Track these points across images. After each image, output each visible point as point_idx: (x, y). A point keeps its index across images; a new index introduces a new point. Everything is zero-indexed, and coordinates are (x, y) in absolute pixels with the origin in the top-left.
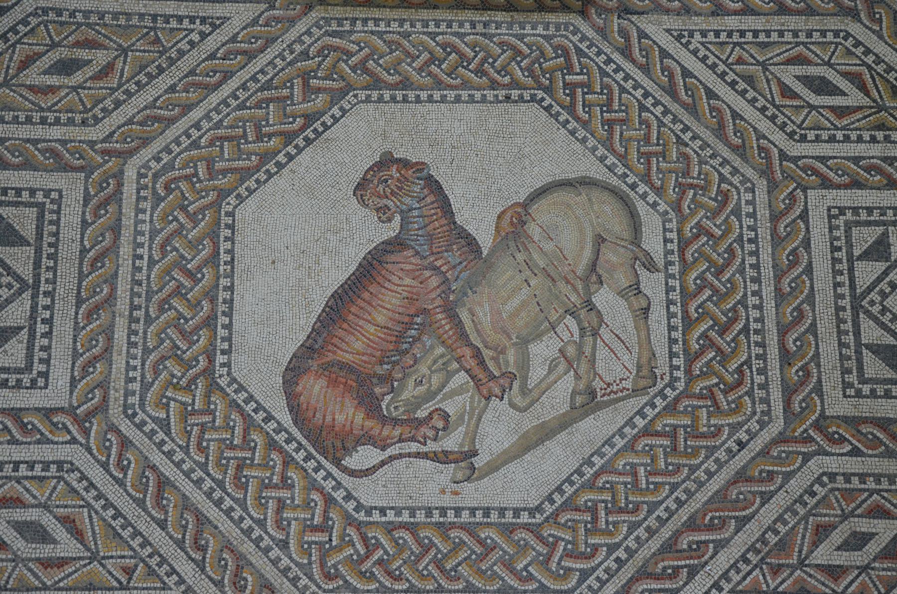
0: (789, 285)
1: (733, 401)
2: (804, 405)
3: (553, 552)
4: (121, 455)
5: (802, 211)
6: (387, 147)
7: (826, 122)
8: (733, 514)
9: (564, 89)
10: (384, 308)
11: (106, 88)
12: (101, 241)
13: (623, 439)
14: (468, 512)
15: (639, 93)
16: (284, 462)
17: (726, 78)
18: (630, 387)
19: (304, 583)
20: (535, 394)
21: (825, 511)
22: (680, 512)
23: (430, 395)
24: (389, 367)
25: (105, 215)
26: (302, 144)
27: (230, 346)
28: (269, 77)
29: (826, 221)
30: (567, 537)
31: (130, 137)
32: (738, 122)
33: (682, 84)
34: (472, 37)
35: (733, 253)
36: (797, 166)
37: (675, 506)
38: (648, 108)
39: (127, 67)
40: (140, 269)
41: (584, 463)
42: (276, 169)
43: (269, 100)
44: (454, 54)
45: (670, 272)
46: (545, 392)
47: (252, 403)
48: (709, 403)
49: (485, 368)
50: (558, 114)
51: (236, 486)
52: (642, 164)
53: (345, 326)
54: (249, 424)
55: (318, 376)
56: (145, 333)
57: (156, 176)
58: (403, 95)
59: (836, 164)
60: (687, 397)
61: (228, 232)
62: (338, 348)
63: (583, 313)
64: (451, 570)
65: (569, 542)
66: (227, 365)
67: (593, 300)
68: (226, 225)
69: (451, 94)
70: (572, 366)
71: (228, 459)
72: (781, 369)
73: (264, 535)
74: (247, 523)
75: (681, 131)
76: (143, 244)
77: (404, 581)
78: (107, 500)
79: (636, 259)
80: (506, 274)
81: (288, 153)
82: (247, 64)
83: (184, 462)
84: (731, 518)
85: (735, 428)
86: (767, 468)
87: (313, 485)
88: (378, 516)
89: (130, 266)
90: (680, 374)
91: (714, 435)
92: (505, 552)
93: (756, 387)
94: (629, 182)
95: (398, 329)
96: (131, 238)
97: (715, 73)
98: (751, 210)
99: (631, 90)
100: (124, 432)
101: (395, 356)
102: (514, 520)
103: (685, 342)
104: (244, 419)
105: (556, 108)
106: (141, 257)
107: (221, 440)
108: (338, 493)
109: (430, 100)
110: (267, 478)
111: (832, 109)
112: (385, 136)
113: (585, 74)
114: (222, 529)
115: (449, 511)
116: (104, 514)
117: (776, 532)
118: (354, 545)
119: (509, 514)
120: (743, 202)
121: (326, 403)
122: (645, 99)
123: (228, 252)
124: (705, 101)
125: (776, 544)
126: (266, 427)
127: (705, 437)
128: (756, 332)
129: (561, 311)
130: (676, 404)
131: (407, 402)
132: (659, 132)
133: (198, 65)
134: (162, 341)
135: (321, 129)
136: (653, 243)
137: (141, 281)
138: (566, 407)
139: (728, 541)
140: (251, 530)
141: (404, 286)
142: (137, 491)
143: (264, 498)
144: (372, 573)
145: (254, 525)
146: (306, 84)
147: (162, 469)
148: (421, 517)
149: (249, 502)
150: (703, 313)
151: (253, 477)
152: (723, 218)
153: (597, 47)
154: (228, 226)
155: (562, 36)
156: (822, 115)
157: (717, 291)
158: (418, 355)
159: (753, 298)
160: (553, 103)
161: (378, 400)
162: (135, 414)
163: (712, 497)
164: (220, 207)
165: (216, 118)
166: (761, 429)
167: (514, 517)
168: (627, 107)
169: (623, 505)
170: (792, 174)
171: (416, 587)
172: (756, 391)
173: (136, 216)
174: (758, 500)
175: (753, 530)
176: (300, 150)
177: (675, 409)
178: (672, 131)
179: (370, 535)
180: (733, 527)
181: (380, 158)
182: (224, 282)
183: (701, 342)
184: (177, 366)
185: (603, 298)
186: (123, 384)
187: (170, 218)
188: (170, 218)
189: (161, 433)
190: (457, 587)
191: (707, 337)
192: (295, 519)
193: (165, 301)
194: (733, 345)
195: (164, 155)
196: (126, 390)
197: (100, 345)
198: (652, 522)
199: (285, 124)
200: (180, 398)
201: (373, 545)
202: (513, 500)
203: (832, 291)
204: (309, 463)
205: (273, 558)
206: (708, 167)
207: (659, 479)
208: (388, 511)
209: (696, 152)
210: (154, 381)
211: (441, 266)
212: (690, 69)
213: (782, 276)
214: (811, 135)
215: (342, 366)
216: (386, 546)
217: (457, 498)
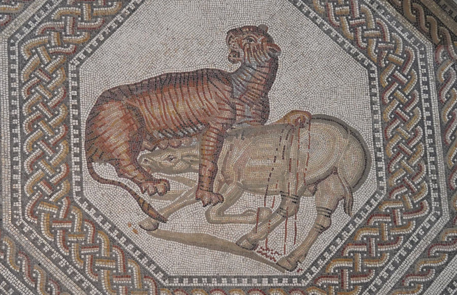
0: (410, 283)
5: (453, 251)
6: (269, 24)
9: (389, 77)
13: (248, 283)
14: (133, 247)
16: (64, 136)
18: (277, 260)
19: (17, 205)
20: (224, 219)
23: (169, 171)
24: (162, 137)
27: (92, 53)
34: (366, 7)
35: (398, 240)
38: (424, 126)
41: (216, 277)
44: (348, 7)
45: (355, 220)
46: (230, 222)
47: (76, 92)
49: (211, 183)
50: (374, 86)
52: (394, 152)
53: (159, 95)
54: (64, 101)
55: (121, 108)
56: (56, 8)
58: (302, 5)
62: (145, 103)
63: (289, 200)
64: (97, 267)
67: (301, 199)
69: (327, 26)
70: (257, 222)
71: (38, 109)
73: (20, 163)
74: (17, 149)
75: (430, 153)
77: (68, 251)
79: (343, 198)
80: (268, 145)
83: (15, 91)
88: (85, 206)
92: (133, 283)
94: (378, 155)
95: (185, 122)
98: (427, 227)
99: (424, 109)
102: (152, 272)
104: (64, 96)
105: (376, 83)
108: (76, 177)
109: (314, 20)
110: (48, 136)
113: (408, 79)
115: (123, 237)
118: (59, 210)
119: (153, 267)
120: (427, 219)
122: (427, 120)
126: (71, 110)
130: (293, 290)
131: (154, 163)
134: (60, 20)
136: (360, 198)
138: (234, 241)
140: (16, 154)
141: (209, 102)
143: (37, 145)
144: (56, 232)
145: (19, 153)
149: (27, 140)
150: (352, 257)
151: (41, 129)
152: (409, 218)
153: (427, 71)
155: (414, 48)
157: (370, 253)
158: (183, 145)
159: (385, 273)
160: (377, 79)
161: (141, 148)
162: (13, 45)
167: (153, 271)
168: (413, 115)
171: (72, 259)
178: (426, 149)
179: (72, 212)
182: (119, 18)
183: (337, 271)
184: (56, 39)
185: (308, 203)
186: (21, 24)
189: (17, 66)
190: (91, 278)
191: (342, 271)
192: (43, 170)
194: (352, 287)
196: (20, 28)
200: (42, 57)
204: (75, 148)
205: (14, 178)
206: (426, 184)
208: (92, 209)
209: (427, 171)
210: (38, 36)
211: (238, 110)
213: (411, 275)
215: (139, 114)
216: (75, 225)
217: (134, 235)
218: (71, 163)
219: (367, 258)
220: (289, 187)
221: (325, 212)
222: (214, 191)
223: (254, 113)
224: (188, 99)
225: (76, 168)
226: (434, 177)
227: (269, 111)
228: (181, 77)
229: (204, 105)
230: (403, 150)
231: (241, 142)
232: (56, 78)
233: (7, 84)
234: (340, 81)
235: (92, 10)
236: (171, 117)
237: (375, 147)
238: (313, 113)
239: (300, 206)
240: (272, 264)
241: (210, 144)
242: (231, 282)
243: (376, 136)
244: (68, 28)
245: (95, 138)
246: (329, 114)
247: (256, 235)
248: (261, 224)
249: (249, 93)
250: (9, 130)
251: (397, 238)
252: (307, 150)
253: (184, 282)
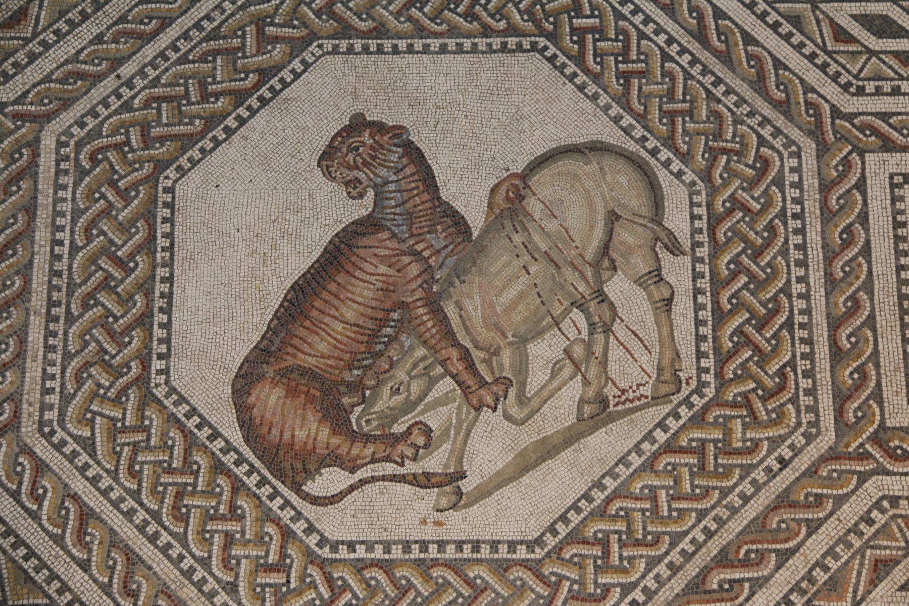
0: (842, 268)
1: (774, 410)
2: (860, 414)
3: (555, 594)
4: (35, 482)
6: (359, 107)
7: (889, 71)
8: (774, 546)
9: (572, 36)
10: (354, 301)
11: (19, 39)
12: (13, 224)
13: (640, 456)
15: (661, 39)
16: (233, 488)
17: (768, 19)
20: (535, 403)
21: (885, 543)
22: (709, 544)
23: (409, 406)
25: (17, 192)
26: (255, 104)
27: (169, 349)
28: (216, 24)
29: (888, 190)
30: (573, 576)
31: (47, 97)
32: (781, 72)
33: (713, 27)
36: (853, 125)
37: (704, 537)
39: (43, 13)
40: (59, 258)
41: (593, 486)
42: (224, 136)
43: (216, 53)
45: (698, 255)
47: (195, 418)
48: (745, 413)
49: (475, 372)
50: (564, 66)
51: (174, 517)
52: (664, 125)
55: (274, 384)
56: (66, 334)
57: (79, 145)
58: (378, 45)
59: (900, 121)
60: (718, 405)
61: (167, 212)
62: (299, 350)
63: (592, 306)
65: (574, 582)
66: (165, 372)
67: (606, 289)
68: (164, 203)
69: (435, 44)
70: (579, 369)
71: (166, 485)
72: (831, 371)
73: (208, 577)
74: (188, 562)
76: (64, 227)
78: (17, 536)
79: (656, 240)
80: (501, 261)
81: (239, 116)
82: (189, 9)
83: (112, 489)
84: (770, 551)
85: (775, 443)
86: (814, 491)
87: (268, 515)
89: (48, 254)
90: (709, 378)
91: (750, 451)
92: (497, 594)
93: (801, 393)
94: (649, 147)
96: (49, 220)
97: (754, 13)
98: (796, 179)
99: (652, 35)
100: (40, 454)
101: (367, 359)
103: (715, 339)
104: (185, 437)
105: (562, 59)
106: (61, 243)
107: (156, 462)
108: (298, 524)
109: (410, 50)
110: (212, 507)
111: (896, 54)
112: (355, 95)
113: (597, 17)
114: (157, 570)
115: (430, 546)
116: (14, 554)
117: (826, 569)
118: (316, 588)
119: (503, 548)
120: (787, 170)
121: (283, 416)
122: (669, 46)
123: (165, 236)
124: (741, 47)
125: (825, 583)
127: (740, 453)
128: (802, 326)
129: (566, 303)
130: (704, 414)
131: (381, 415)
132: (685, 86)
133: (130, 10)
134: (86, 344)
135: (278, 87)
136: (677, 220)
137: (61, 271)
138: (572, 419)
139: (767, 579)
140: (192, 570)
142: (55, 526)
143: (208, 532)
145: (196, 565)
146: (260, 32)
147: (86, 499)
148: (397, 552)
149: (190, 538)
150: (737, 304)
152: (762, 189)
154: (166, 205)
156: (884, 62)
157: (755, 277)
158: (395, 358)
159: (799, 286)
162: (53, 433)
163: (748, 526)
164: (157, 181)
165: (152, 73)
166: (808, 444)
167: (508, 552)
168: (647, 56)
169: (640, 537)
170: (847, 135)
172: (801, 398)
173: (55, 193)
174: (804, 530)
175: (797, 567)
176: (253, 112)
177: (703, 420)
178: (701, 84)
179: (335, 575)
180: (773, 563)
182: (161, 272)
183: (735, 339)
184: (104, 374)
185: (619, 288)
186: (38, 396)
187: (97, 195)
188: (97, 195)
189: (84, 455)
191: (742, 332)
192: (246, 557)
193: (91, 295)
194: (773, 342)
195: (89, 120)
196: (42, 403)
197: (11, 349)
198: (675, 556)
199: (235, 80)
200: (108, 412)
201: (339, 587)
202: (510, 533)
203: (894, 276)
204: (263, 490)
206: (744, 128)
207: (684, 505)
209: (730, 110)
210: (76, 392)
212: (724, 9)
214: (870, 87)
215: (304, 371)
218: (276, 514)
219: (756, 288)
222: (489, 379)
224: (348, 294)
225: (287, 514)
226: (745, 109)
231: (465, 288)
232: (151, 423)
233: (93, 490)
234: (515, 98)
235: (117, 294)
237: (636, 141)
240: (647, 405)
242: (618, 476)
244: (106, 346)
245: (277, 453)
250: (152, 548)
251: (771, 228)
252: (556, 223)
253: (560, 530)
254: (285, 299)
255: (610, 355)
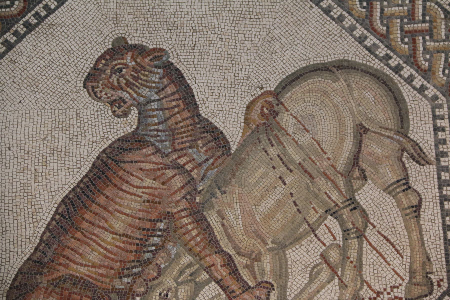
6: (120, 32)
10: (122, 213)
45: (443, 164)
49: (239, 278)
52: (406, 43)
62: (71, 260)
63: (346, 213)
67: (357, 197)
70: (336, 273)
79: (403, 151)
80: (258, 171)
94: (393, 65)
95: (139, 237)
101: (136, 267)
112: (117, 20)
129: (321, 211)
132: (424, 7)
135: (43, 13)
141: (144, 187)
158: (163, 266)
176: (20, 37)
181: (113, 45)
185: (369, 196)
211: (184, 165)
215: (76, 281)
220: (330, 198)
221: (398, 187)
222: (251, 284)
223: (206, 151)
224: (117, 207)
227: (222, 133)
228: (82, 189)
229: (141, 197)
230: (416, 31)
231: (226, 198)
234: (266, 22)
236: (117, 246)
238: (272, 86)
239: (364, 207)
241: (194, 234)
243: (369, 45)
246: (292, 70)
247: (350, 290)
248: (342, 272)
249: (178, 134)
252: (308, 136)
254: (56, 212)
255: (364, 259)
